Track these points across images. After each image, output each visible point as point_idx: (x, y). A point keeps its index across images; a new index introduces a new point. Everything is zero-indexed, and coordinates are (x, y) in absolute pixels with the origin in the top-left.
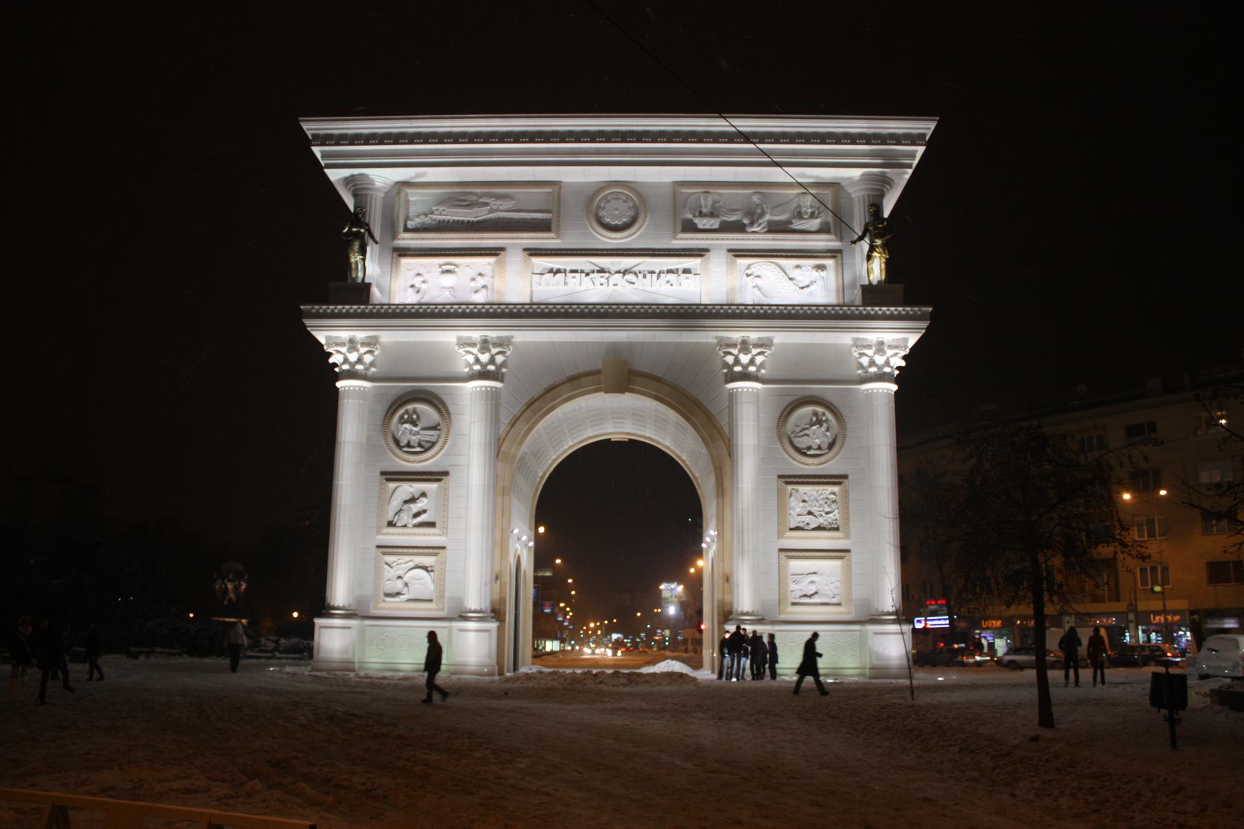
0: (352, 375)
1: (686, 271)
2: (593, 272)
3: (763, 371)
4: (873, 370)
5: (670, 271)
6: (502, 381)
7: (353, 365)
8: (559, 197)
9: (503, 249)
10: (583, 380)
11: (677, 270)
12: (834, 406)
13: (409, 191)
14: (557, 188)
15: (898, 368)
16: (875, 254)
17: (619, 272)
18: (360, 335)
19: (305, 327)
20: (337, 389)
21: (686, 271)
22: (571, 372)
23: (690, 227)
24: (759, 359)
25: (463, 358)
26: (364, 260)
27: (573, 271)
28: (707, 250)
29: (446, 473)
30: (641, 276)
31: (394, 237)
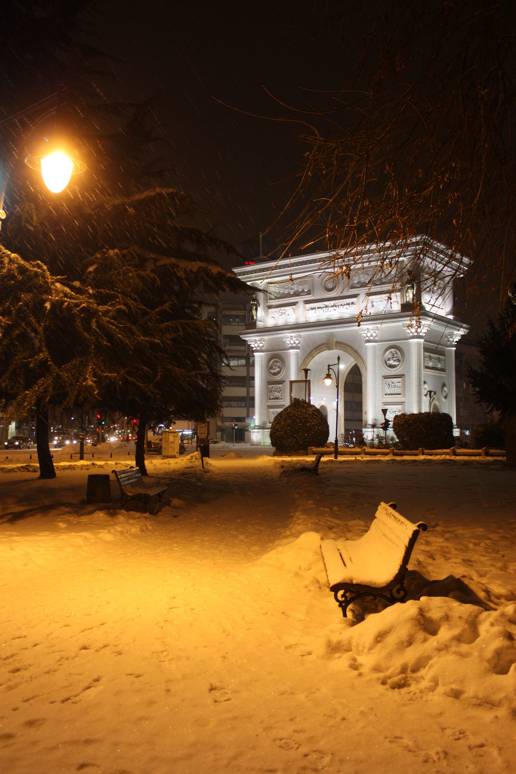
0: (257, 351)
1: (352, 303)
2: (323, 307)
3: (377, 338)
4: (411, 334)
5: (348, 304)
6: (299, 349)
7: (256, 347)
8: (313, 281)
9: (297, 302)
10: (322, 346)
11: (349, 303)
12: (401, 349)
13: (271, 285)
14: (312, 278)
15: (425, 333)
16: (409, 290)
17: (332, 306)
18: (257, 338)
19: (240, 337)
20: (254, 356)
21: (352, 303)
22: (319, 344)
23: (353, 287)
24: (374, 335)
25: (287, 342)
26: (256, 313)
27: (318, 308)
28: (359, 295)
29: (284, 381)
30: (337, 307)
31: (267, 302)
